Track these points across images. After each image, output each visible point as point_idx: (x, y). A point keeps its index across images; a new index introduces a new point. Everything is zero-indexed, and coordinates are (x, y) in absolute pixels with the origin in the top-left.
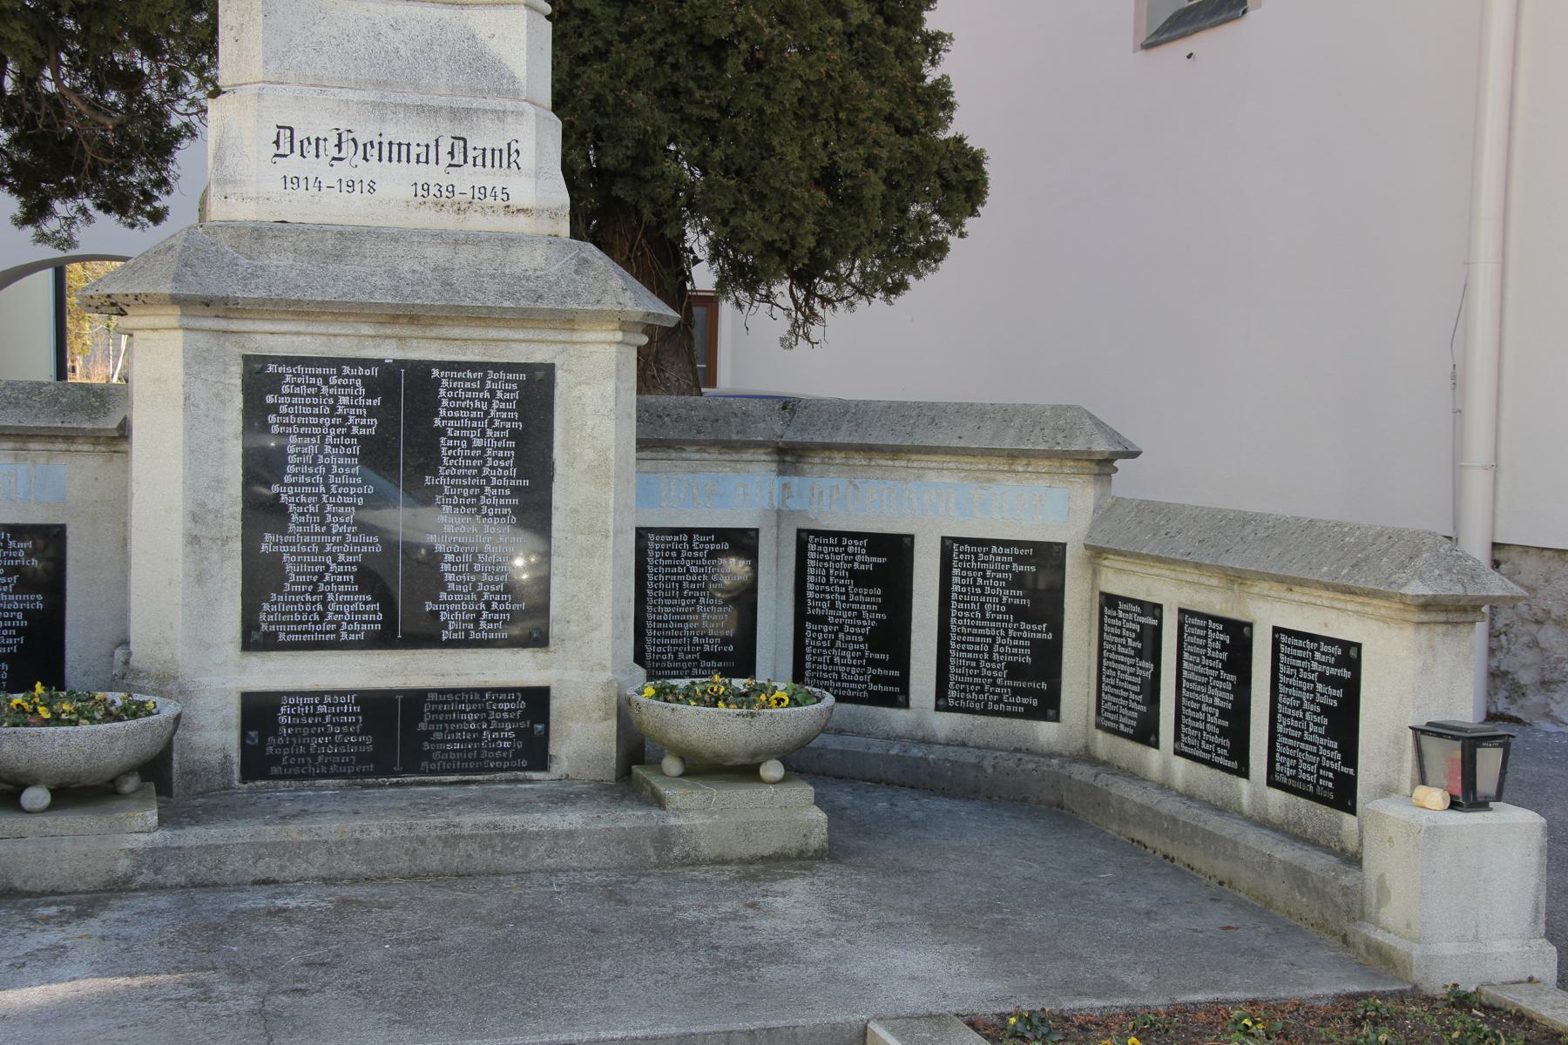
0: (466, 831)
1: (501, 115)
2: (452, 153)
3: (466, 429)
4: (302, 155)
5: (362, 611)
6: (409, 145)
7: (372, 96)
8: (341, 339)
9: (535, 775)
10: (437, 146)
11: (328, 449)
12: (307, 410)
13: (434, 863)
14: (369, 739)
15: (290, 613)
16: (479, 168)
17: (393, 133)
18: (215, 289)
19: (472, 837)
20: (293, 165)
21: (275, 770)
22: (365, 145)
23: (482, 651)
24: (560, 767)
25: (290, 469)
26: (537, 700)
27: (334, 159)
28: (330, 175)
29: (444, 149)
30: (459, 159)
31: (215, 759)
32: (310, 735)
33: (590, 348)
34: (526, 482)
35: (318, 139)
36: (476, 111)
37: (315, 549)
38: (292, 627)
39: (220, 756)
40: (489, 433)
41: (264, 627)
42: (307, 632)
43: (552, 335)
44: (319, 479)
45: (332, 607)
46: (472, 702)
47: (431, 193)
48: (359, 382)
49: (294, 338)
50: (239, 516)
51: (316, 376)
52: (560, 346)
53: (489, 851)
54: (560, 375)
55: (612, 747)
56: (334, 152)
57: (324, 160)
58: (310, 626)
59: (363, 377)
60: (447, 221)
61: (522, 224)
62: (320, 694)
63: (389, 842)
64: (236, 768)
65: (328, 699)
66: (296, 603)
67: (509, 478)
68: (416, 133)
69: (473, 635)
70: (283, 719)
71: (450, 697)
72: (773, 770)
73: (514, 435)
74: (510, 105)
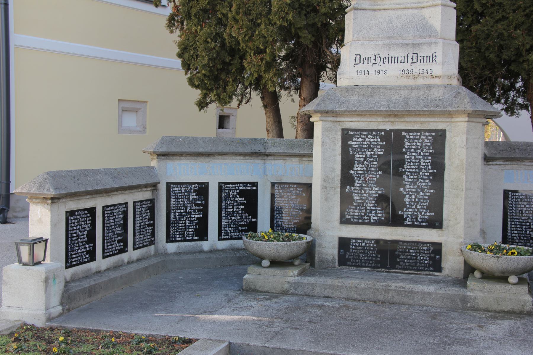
0: (392, 288)
1: (430, 44)
2: (412, 59)
3: (414, 152)
4: (363, 63)
6: (398, 57)
7: (386, 42)
8: (373, 123)
9: (436, 274)
10: (408, 57)
11: (367, 159)
12: (361, 146)
13: (381, 298)
14: (379, 256)
15: (355, 212)
16: (422, 63)
17: (393, 54)
18: (329, 108)
19: (394, 290)
20: (361, 67)
21: (349, 263)
22: (383, 58)
23: (419, 229)
24: (445, 272)
25: (356, 165)
27: (373, 64)
28: (372, 69)
30: (415, 60)
31: (330, 258)
32: (360, 253)
33: (459, 124)
34: (435, 171)
35: (368, 58)
36: (421, 43)
37: (363, 192)
38: (355, 217)
39: (332, 257)
40: (422, 154)
41: (347, 216)
42: (360, 219)
43: (444, 120)
44: (365, 169)
45: (368, 211)
46: (414, 246)
47: (405, 73)
48: (378, 137)
49: (358, 123)
50: (340, 180)
51: (364, 135)
52: (448, 123)
53: (400, 296)
54: (447, 133)
55: (462, 266)
56: (373, 62)
57: (370, 64)
58: (361, 217)
59: (379, 135)
60: (411, 82)
61: (437, 81)
62: (363, 239)
63: (367, 289)
64: (337, 261)
65: (366, 241)
66: (357, 209)
67: (429, 169)
68: (400, 53)
69: (415, 223)
70: (351, 247)
71: (406, 244)
72: (513, 279)
73: (431, 154)
74: (433, 40)
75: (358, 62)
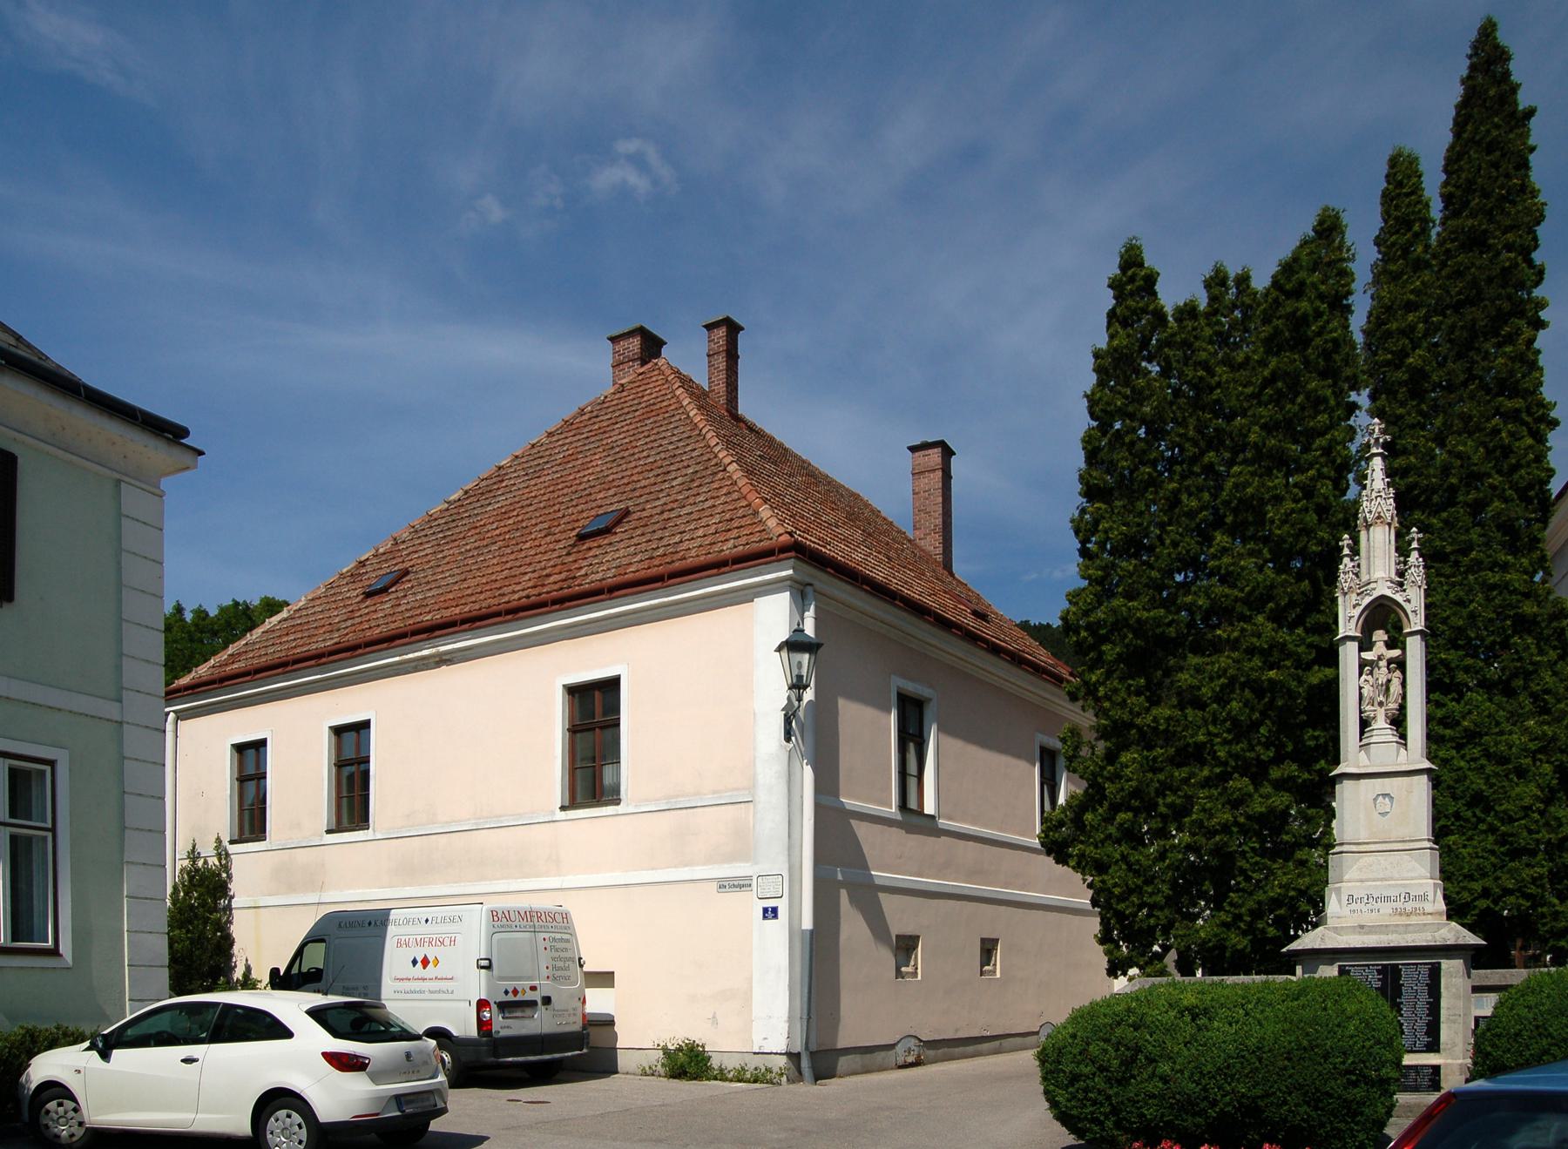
26: (1436, 1069)
28: (1365, 909)
60: (1403, 920)
61: (1429, 919)
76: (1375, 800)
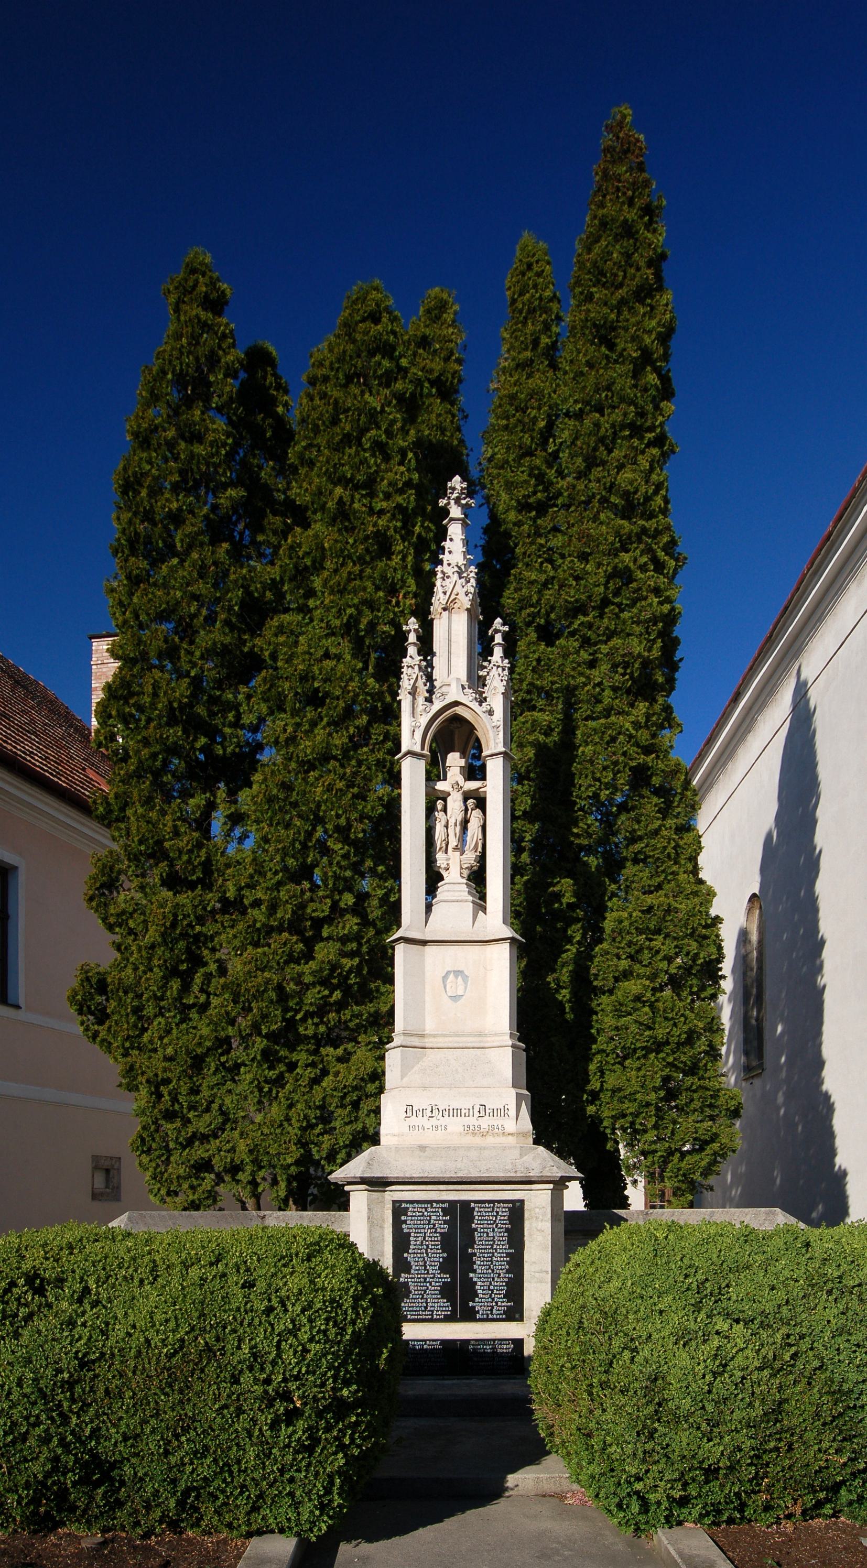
5: (442, 1306)
20: (414, 1120)
28: (428, 1124)
29: (476, 1110)
30: (482, 1113)
57: (426, 1118)
62: (425, 1341)
73: (507, 1230)
75: (409, 1114)
76: (445, 978)
